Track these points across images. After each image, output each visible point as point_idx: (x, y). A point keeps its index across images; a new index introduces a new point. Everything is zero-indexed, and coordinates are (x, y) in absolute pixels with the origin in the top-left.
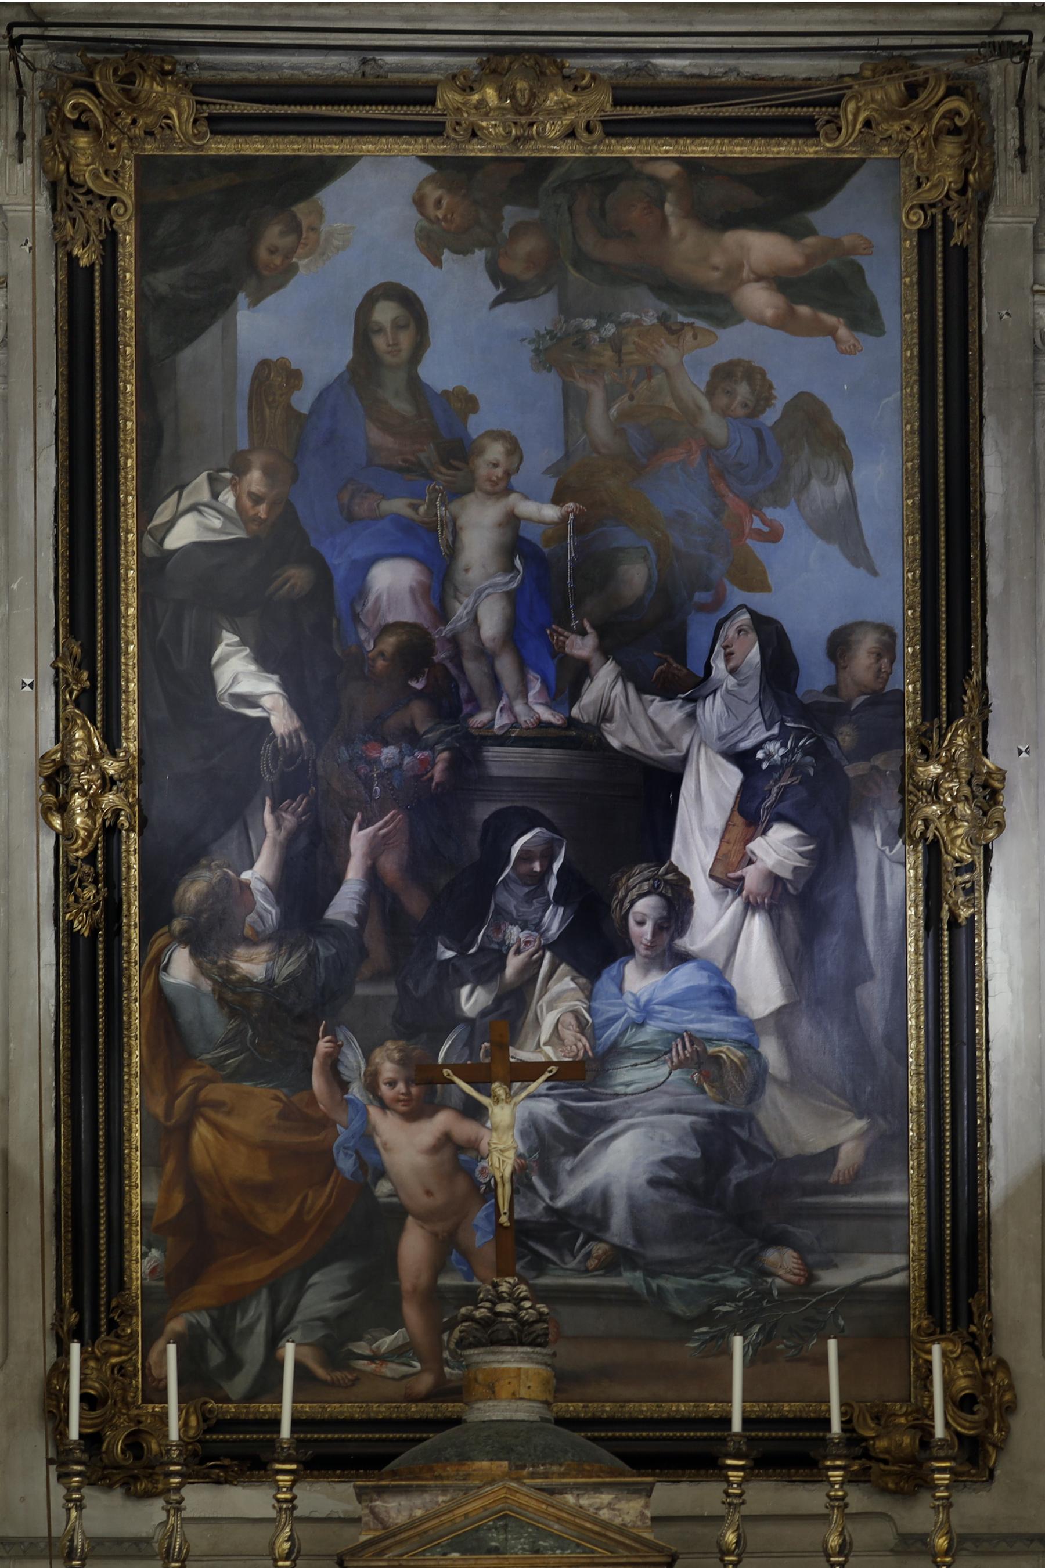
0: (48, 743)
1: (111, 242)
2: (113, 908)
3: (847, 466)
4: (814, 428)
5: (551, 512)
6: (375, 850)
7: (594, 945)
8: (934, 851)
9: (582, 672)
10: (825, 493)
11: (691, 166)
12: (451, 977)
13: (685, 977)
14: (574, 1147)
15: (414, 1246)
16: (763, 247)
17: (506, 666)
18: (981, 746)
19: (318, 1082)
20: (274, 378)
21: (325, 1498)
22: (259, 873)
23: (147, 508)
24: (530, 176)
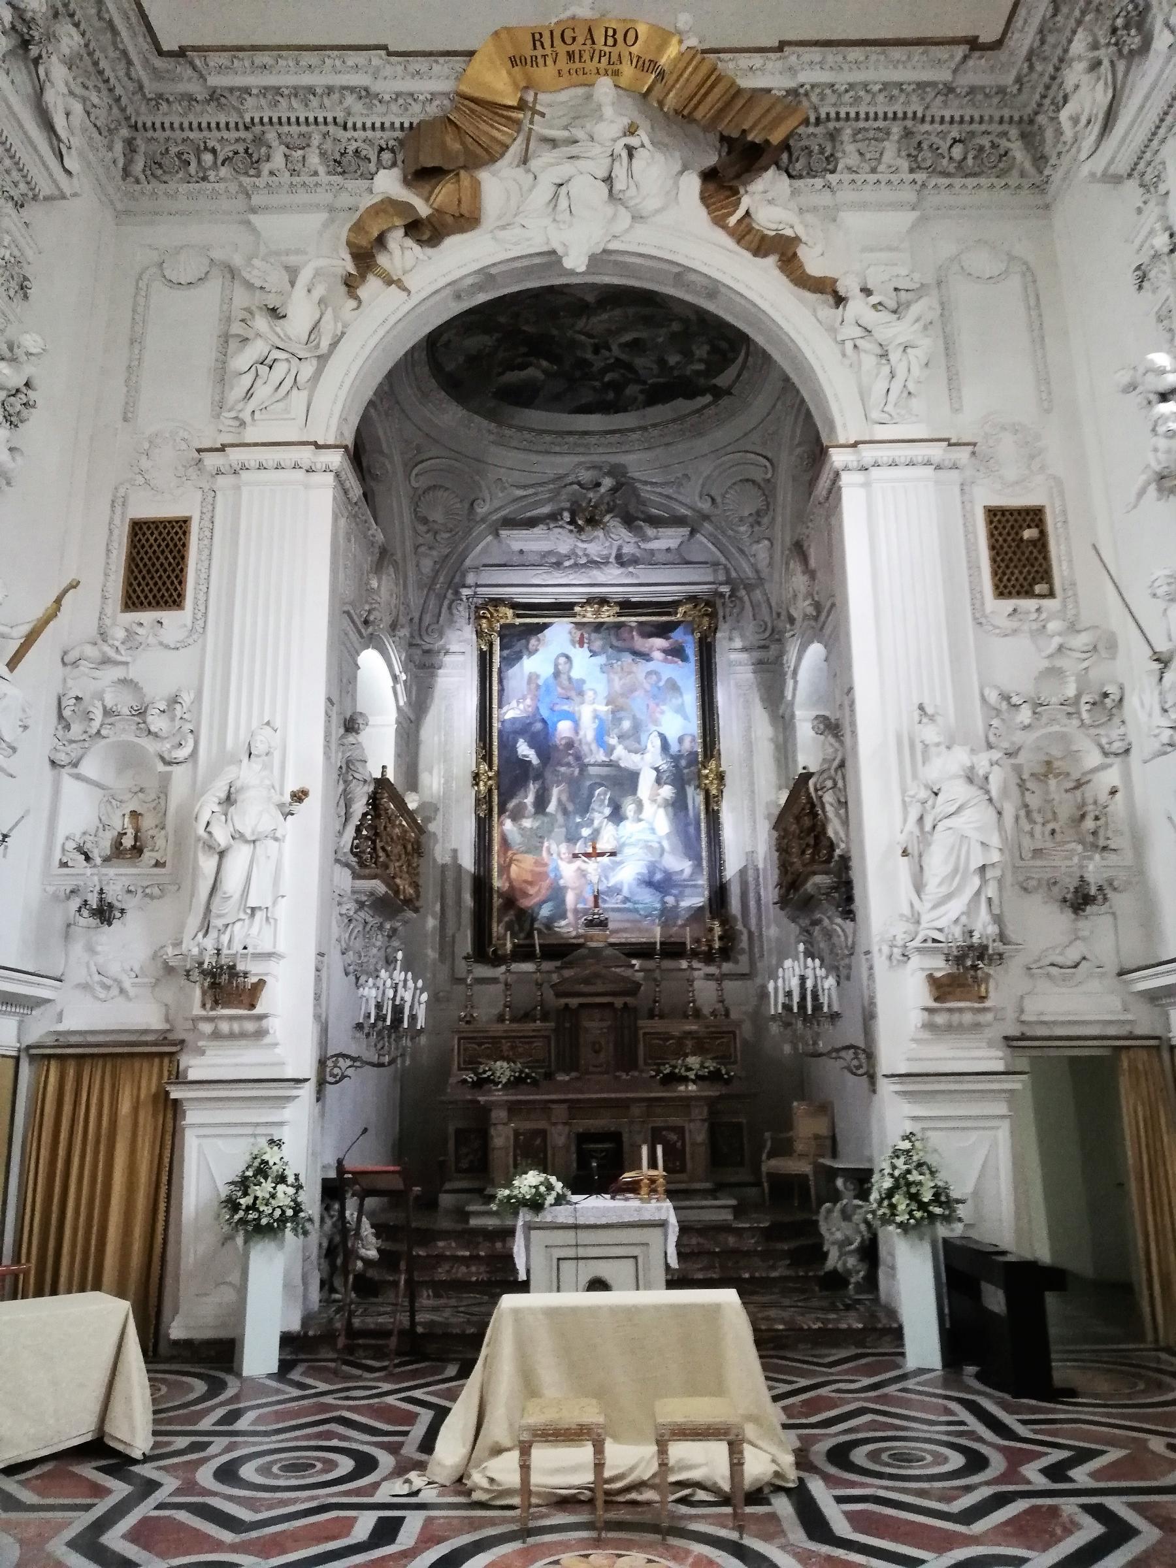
0: (474, 768)
1: (491, 645)
2: (490, 810)
3: (681, 694)
4: (673, 686)
5: (606, 708)
6: (560, 792)
7: (617, 815)
8: (707, 792)
9: (613, 749)
10: (676, 701)
11: (640, 623)
12: (579, 826)
13: (642, 825)
14: (613, 869)
15: (570, 899)
16: (659, 642)
17: (594, 747)
18: (719, 765)
19: (544, 854)
20: (532, 678)
21: (547, 966)
22: (530, 800)
23: (500, 706)
24: (598, 627)
